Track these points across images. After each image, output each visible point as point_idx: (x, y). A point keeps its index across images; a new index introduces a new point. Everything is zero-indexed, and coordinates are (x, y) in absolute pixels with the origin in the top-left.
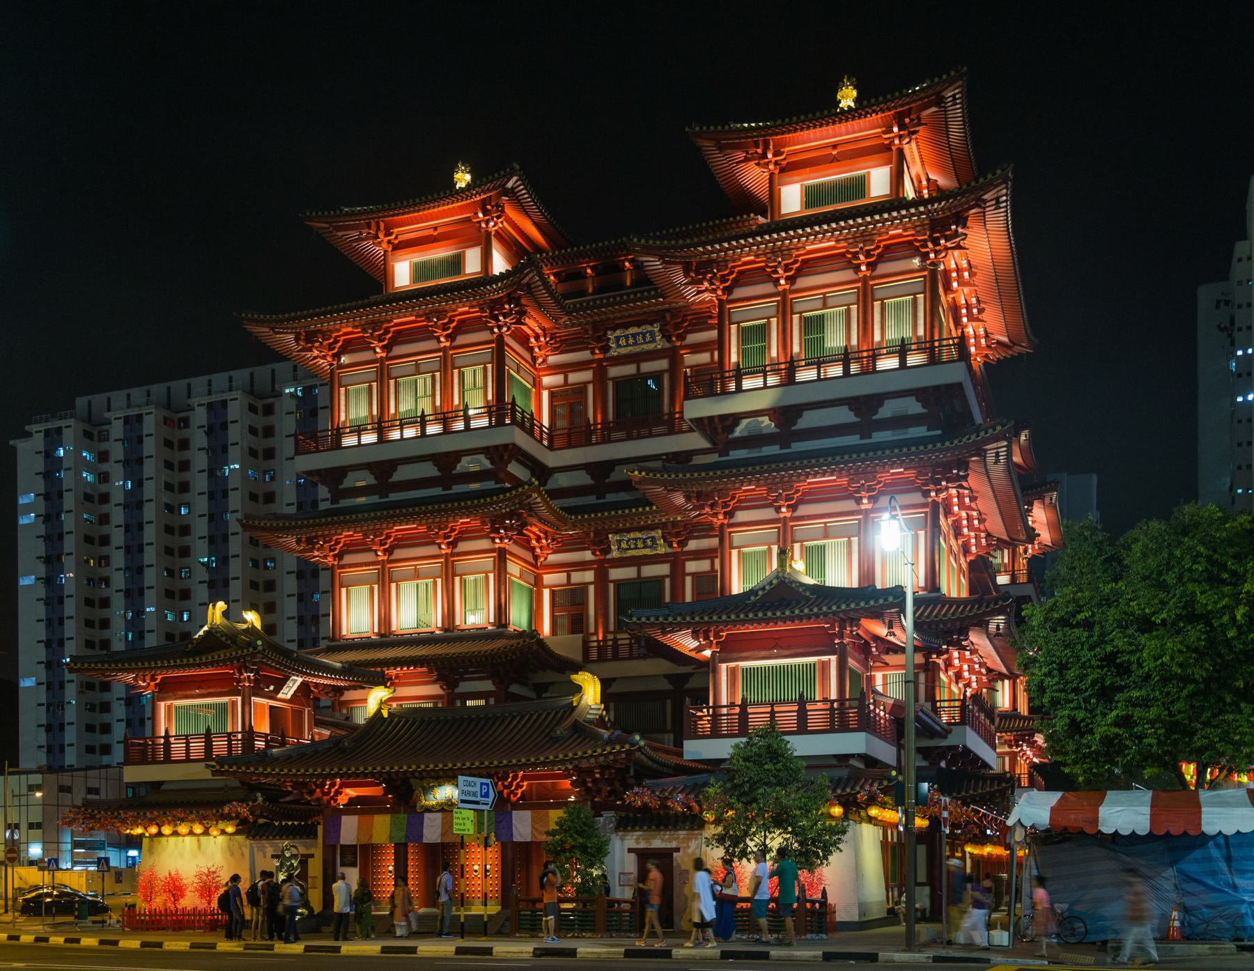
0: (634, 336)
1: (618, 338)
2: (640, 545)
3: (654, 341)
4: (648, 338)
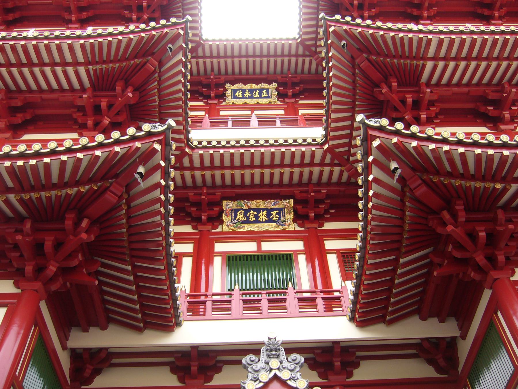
0: (251, 91)
1: (234, 91)
2: (263, 215)
3: (268, 97)
4: (264, 94)
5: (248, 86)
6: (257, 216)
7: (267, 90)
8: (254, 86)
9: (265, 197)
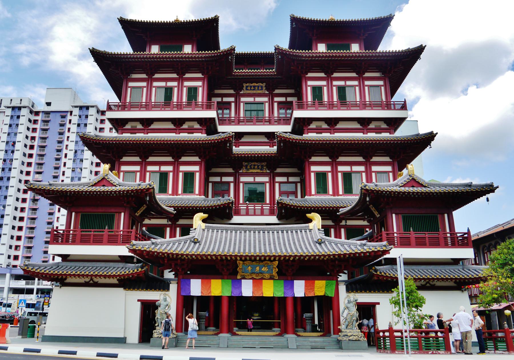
0: (254, 87)
1: (247, 87)
3: (262, 89)
5: (253, 84)
6: (254, 167)
7: (262, 87)
8: (255, 84)
9: (257, 162)
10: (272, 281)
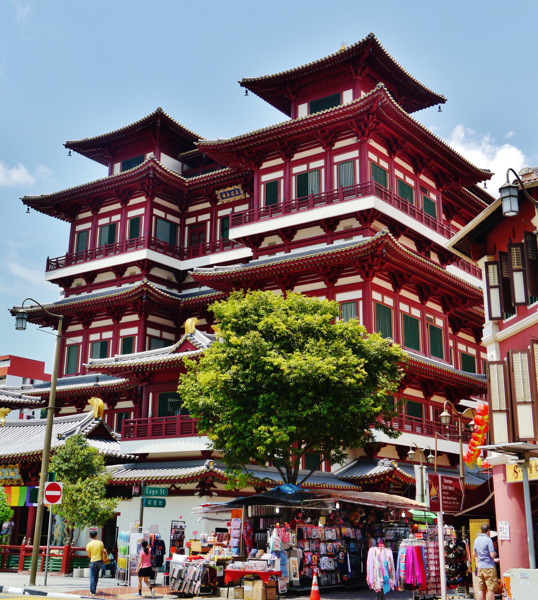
0: (230, 192)
1: (221, 194)
3: (240, 194)
8: (230, 189)
10: (19, 487)
